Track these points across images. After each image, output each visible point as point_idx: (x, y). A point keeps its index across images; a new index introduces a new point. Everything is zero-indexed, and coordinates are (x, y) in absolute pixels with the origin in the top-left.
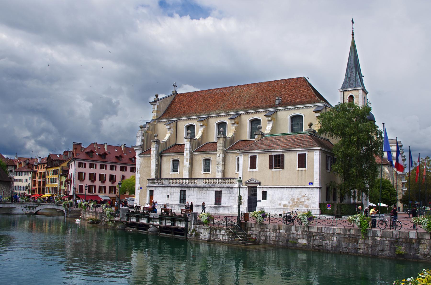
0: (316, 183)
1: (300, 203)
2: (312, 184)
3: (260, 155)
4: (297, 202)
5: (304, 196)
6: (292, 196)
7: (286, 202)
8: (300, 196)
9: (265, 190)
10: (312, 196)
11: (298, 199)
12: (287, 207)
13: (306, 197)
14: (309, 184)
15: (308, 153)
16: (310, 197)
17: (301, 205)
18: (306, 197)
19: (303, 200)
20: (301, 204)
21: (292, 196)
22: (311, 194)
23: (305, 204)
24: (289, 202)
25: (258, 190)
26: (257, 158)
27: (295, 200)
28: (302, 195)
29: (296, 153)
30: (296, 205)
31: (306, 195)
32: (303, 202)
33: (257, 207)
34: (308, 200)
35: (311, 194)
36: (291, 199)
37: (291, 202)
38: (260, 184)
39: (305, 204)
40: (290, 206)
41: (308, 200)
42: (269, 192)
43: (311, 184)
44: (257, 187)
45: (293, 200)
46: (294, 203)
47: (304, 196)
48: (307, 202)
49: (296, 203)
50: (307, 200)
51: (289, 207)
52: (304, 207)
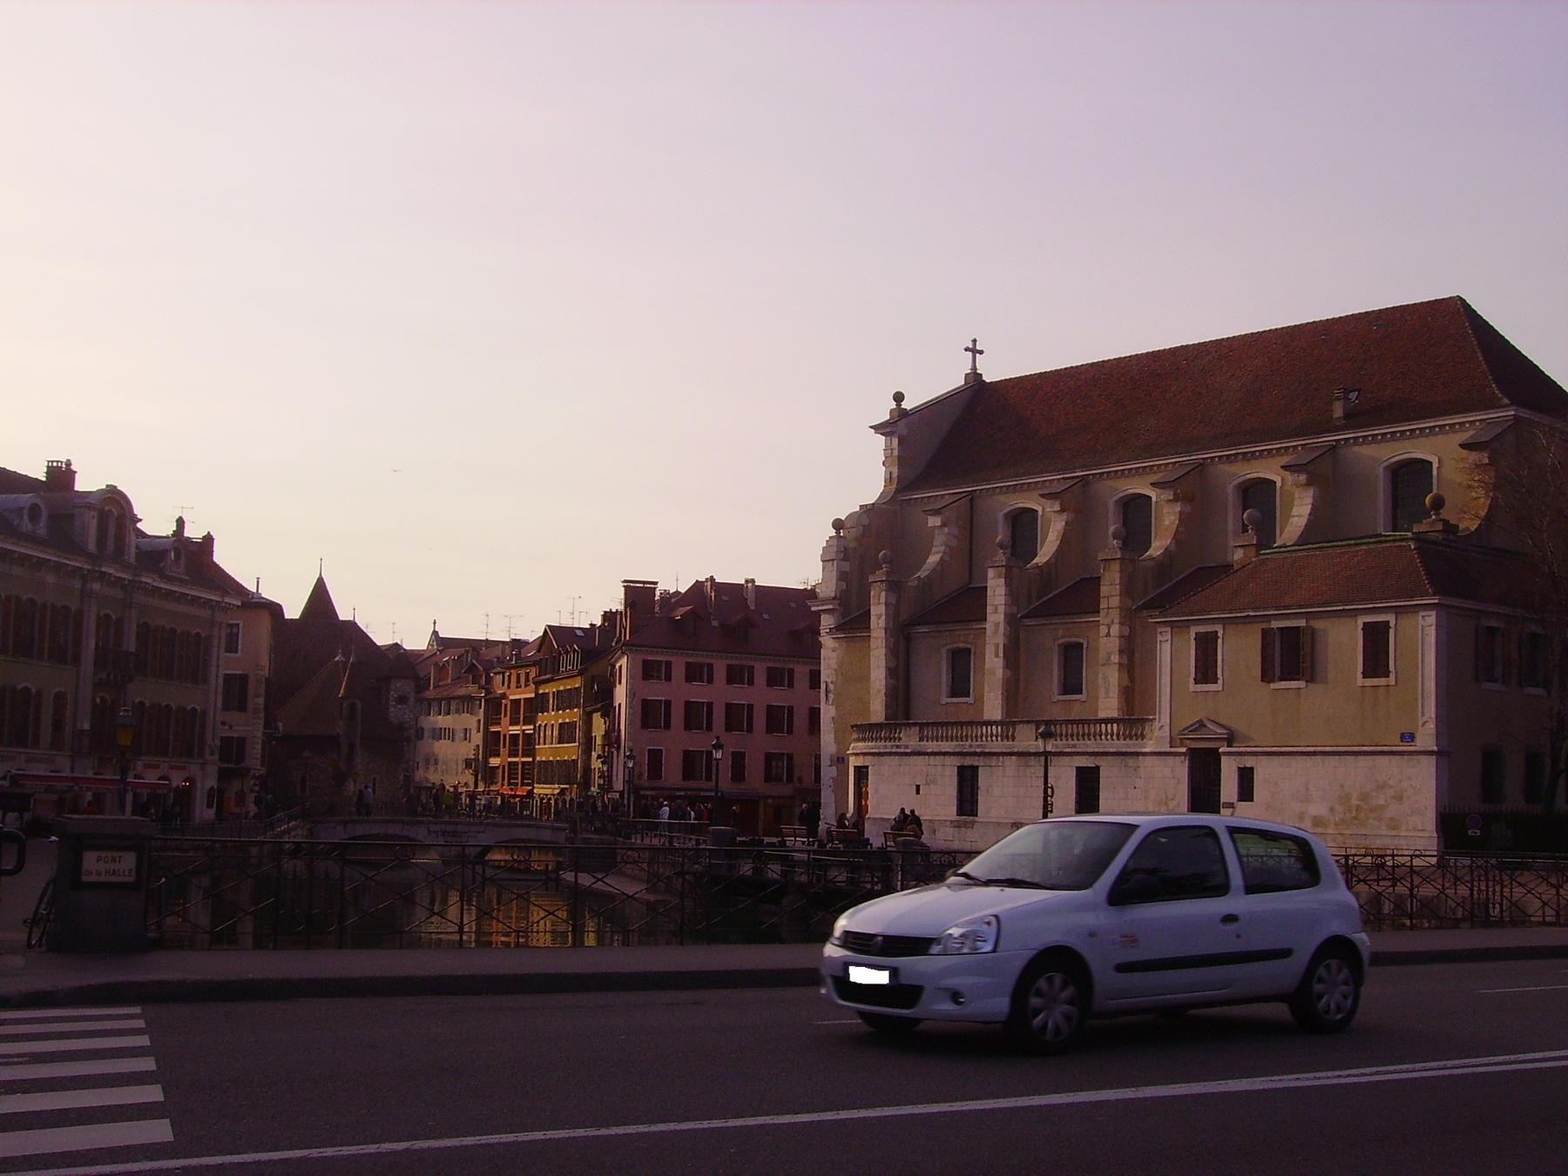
1: (1371, 811)
2: (1412, 737)
4: (1358, 808)
9: (1249, 762)
10: (1412, 786)
11: (1364, 797)
13: (1391, 787)
14: (1402, 737)
16: (1406, 791)
21: (1342, 787)
24: (1332, 809)
27: (1354, 802)
28: (1377, 781)
30: (1355, 818)
31: (1390, 782)
32: (1381, 807)
34: (1399, 798)
36: (1340, 796)
37: (1339, 808)
40: (1337, 824)
41: (1399, 798)
42: (1264, 771)
43: (1409, 737)
46: (1350, 812)
48: (1392, 810)
52: (1384, 828)
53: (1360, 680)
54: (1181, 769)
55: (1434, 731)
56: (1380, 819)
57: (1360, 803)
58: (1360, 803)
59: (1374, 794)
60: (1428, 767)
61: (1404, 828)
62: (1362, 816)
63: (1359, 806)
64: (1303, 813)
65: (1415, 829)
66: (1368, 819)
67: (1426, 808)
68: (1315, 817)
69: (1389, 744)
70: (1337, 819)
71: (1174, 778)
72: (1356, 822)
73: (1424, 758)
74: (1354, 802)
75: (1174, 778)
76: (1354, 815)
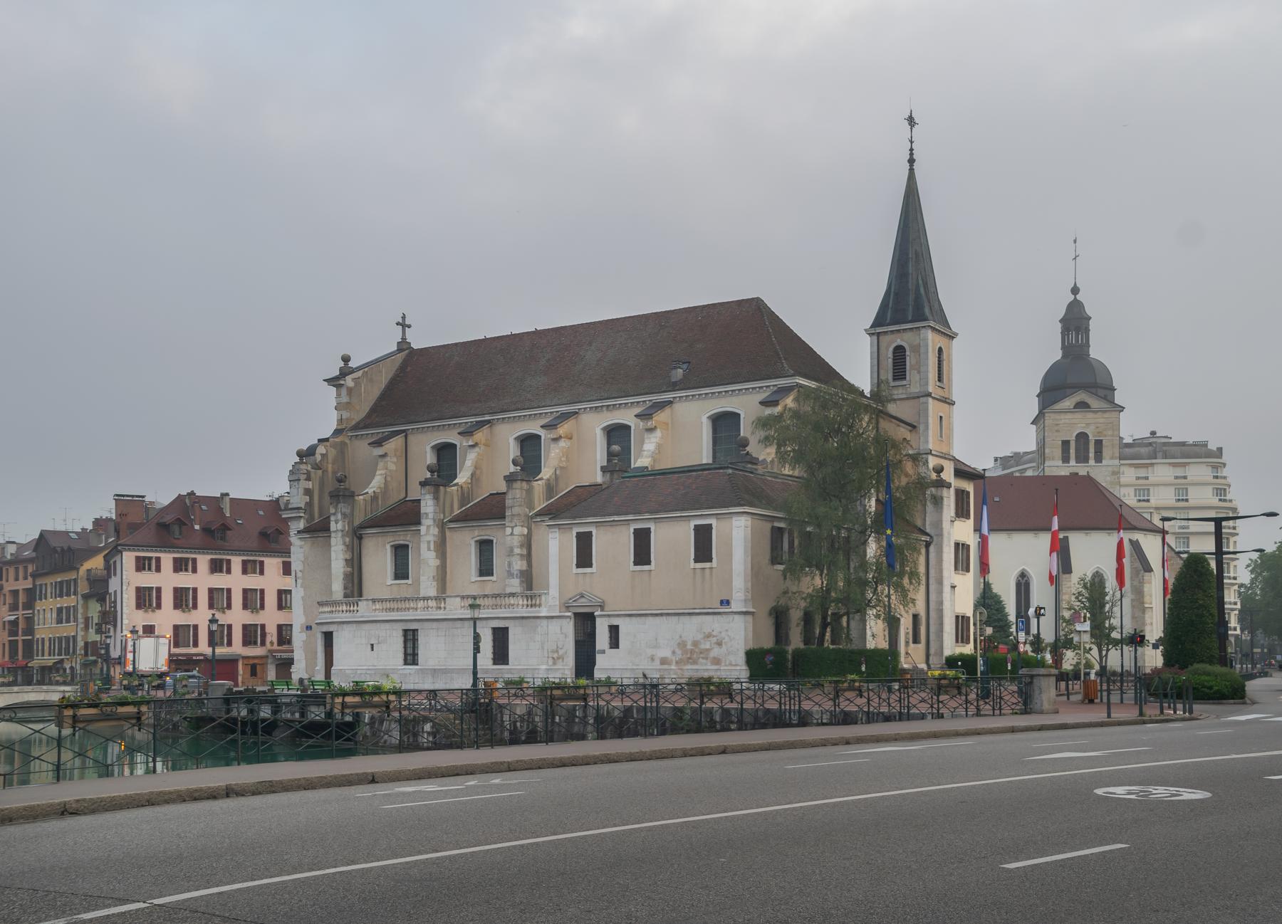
1: (701, 653)
2: (728, 602)
4: (692, 652)
5: (709, 636)
6: (681, 637)
7: (665, 653)
8: (699, 637)
9: (615, 622)
10: (728, 636)
13: (714, 636)
14: (722, 602)
17: (703, 658)
18: (714, 636)
19: (708, 647)
20: (702, 656)
23: (712, 654)
24: (674, 652)
25: (598, 621)
26: (594, 538)
28: (704, 633)
30: (690, 658)
31: (714, 633)
32: (708, 650)
34: (719, 644)
37: (679, 652)
38: (602, 607)
39: (712, 654)
40: (677, 663)
41: (719, 644)
42: (625, 627)
43: (726, 603)
44: (596, 614)
45: (682, 645)
46: (687, 654)
49: (691, 652)
50: (716, 646)
53: (692, 565)
56: (707, 659)
59: (702, 641)
61: (723, 664)
65: (731, 665)
66: (699, 658)
73: (737, 617)
74: (689, 647)
76: (689, 656)
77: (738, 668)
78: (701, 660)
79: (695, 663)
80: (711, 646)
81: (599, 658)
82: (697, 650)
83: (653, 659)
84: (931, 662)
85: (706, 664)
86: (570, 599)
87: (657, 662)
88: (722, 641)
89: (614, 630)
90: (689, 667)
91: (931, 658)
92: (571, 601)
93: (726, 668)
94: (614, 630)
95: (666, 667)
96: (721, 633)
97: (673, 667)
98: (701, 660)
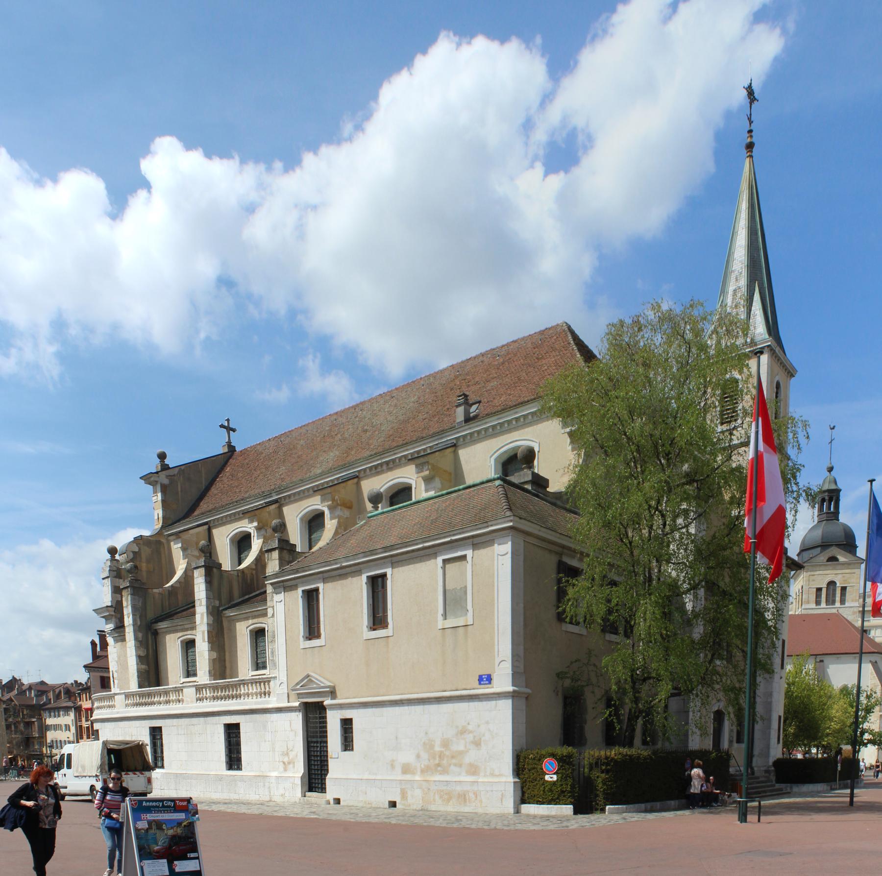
0: (503, 682)
1: (453, 757)
2: (489, 679)
3: (329, 585)
4: (441, 756)
5: (463, 732)
6: (426, 733)
7: (407, 757)
9: (348, 714)
10: (489, 730)
11: (446, 744)
12: (414, 774)
13: (471, 732)
14: (481, 679)
15: (476, 552)
16: (484, 735)
17: (455, 765)
18: (471, 732)
20: (454, 761)
21: (426, 733)
22: (487, 723)
23: (467, 760)
24: (418, 756)
26: (321, 596)
27: (437, 748)
28: (457, 727)
29: (433, 561)
30: (439, 765)
31: (470, 727)
32: (461, 753)
33: (328, 776)
34: (477, 744)
35: (487, 723)
36: (424, 743)
37: (424, 756)
38: (333, 693)
39: (467, 760)
40: (422, 771)
41: (477, 744)
42: (359, 718)
43: (486, 679)
44: (325, 703)
45: (429, 746)
46: (434, 758)
47: (463, 732)
49: (440, 757)
51: (419, 773)
53: (441, 623)
54: (297, 720)
55: (510, 672)
56: (460, 766)
57: (443, 749)
58: (443, 749)
60: (505, 708)
62: (445, 762)
63: (441, 752)
64: (393, 761)
65: (492, 775)
66: (450, 765)
67: (503, 752)
68: (403, 764)
69: (468, 688)
70: (422, 766)
71: (292, 730)
72: (439, 768)
74: (437, 748)
75: (292, 730)
76: (437, 762)
77: (503, 779)
78: (452, 767)
79: (445, 771)
80: (466, 746)
81: (332, 764)
82: (447, 753)
83: (393, 766)
84: (754, 764)
85: (459, 774)
86: (297, 684)
87: (398, 769)
88: (481, 739)
89: (347, 725)
90: (438, 778)
91: (754, 760)
92: (298, 687)
93: (486, 780)
94: (347, 725)
95: (408, 777)
96: (479, 726)
97: (417, 778)
98: (452, 767)
